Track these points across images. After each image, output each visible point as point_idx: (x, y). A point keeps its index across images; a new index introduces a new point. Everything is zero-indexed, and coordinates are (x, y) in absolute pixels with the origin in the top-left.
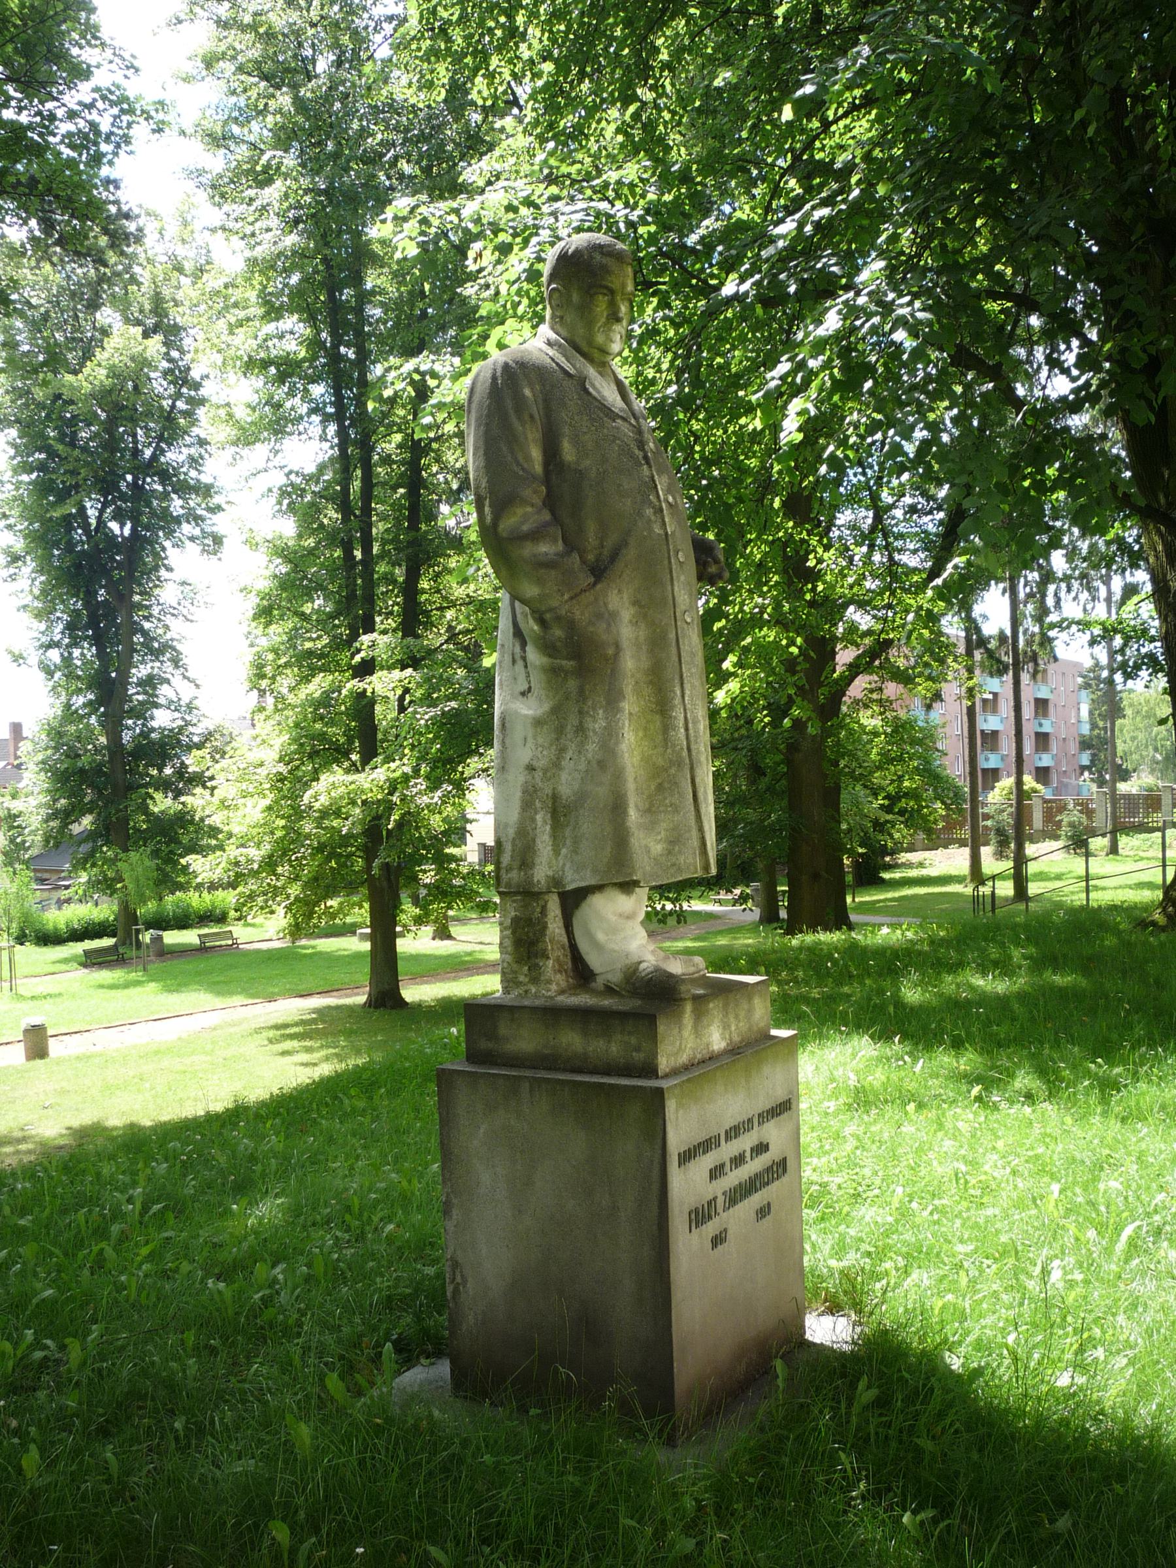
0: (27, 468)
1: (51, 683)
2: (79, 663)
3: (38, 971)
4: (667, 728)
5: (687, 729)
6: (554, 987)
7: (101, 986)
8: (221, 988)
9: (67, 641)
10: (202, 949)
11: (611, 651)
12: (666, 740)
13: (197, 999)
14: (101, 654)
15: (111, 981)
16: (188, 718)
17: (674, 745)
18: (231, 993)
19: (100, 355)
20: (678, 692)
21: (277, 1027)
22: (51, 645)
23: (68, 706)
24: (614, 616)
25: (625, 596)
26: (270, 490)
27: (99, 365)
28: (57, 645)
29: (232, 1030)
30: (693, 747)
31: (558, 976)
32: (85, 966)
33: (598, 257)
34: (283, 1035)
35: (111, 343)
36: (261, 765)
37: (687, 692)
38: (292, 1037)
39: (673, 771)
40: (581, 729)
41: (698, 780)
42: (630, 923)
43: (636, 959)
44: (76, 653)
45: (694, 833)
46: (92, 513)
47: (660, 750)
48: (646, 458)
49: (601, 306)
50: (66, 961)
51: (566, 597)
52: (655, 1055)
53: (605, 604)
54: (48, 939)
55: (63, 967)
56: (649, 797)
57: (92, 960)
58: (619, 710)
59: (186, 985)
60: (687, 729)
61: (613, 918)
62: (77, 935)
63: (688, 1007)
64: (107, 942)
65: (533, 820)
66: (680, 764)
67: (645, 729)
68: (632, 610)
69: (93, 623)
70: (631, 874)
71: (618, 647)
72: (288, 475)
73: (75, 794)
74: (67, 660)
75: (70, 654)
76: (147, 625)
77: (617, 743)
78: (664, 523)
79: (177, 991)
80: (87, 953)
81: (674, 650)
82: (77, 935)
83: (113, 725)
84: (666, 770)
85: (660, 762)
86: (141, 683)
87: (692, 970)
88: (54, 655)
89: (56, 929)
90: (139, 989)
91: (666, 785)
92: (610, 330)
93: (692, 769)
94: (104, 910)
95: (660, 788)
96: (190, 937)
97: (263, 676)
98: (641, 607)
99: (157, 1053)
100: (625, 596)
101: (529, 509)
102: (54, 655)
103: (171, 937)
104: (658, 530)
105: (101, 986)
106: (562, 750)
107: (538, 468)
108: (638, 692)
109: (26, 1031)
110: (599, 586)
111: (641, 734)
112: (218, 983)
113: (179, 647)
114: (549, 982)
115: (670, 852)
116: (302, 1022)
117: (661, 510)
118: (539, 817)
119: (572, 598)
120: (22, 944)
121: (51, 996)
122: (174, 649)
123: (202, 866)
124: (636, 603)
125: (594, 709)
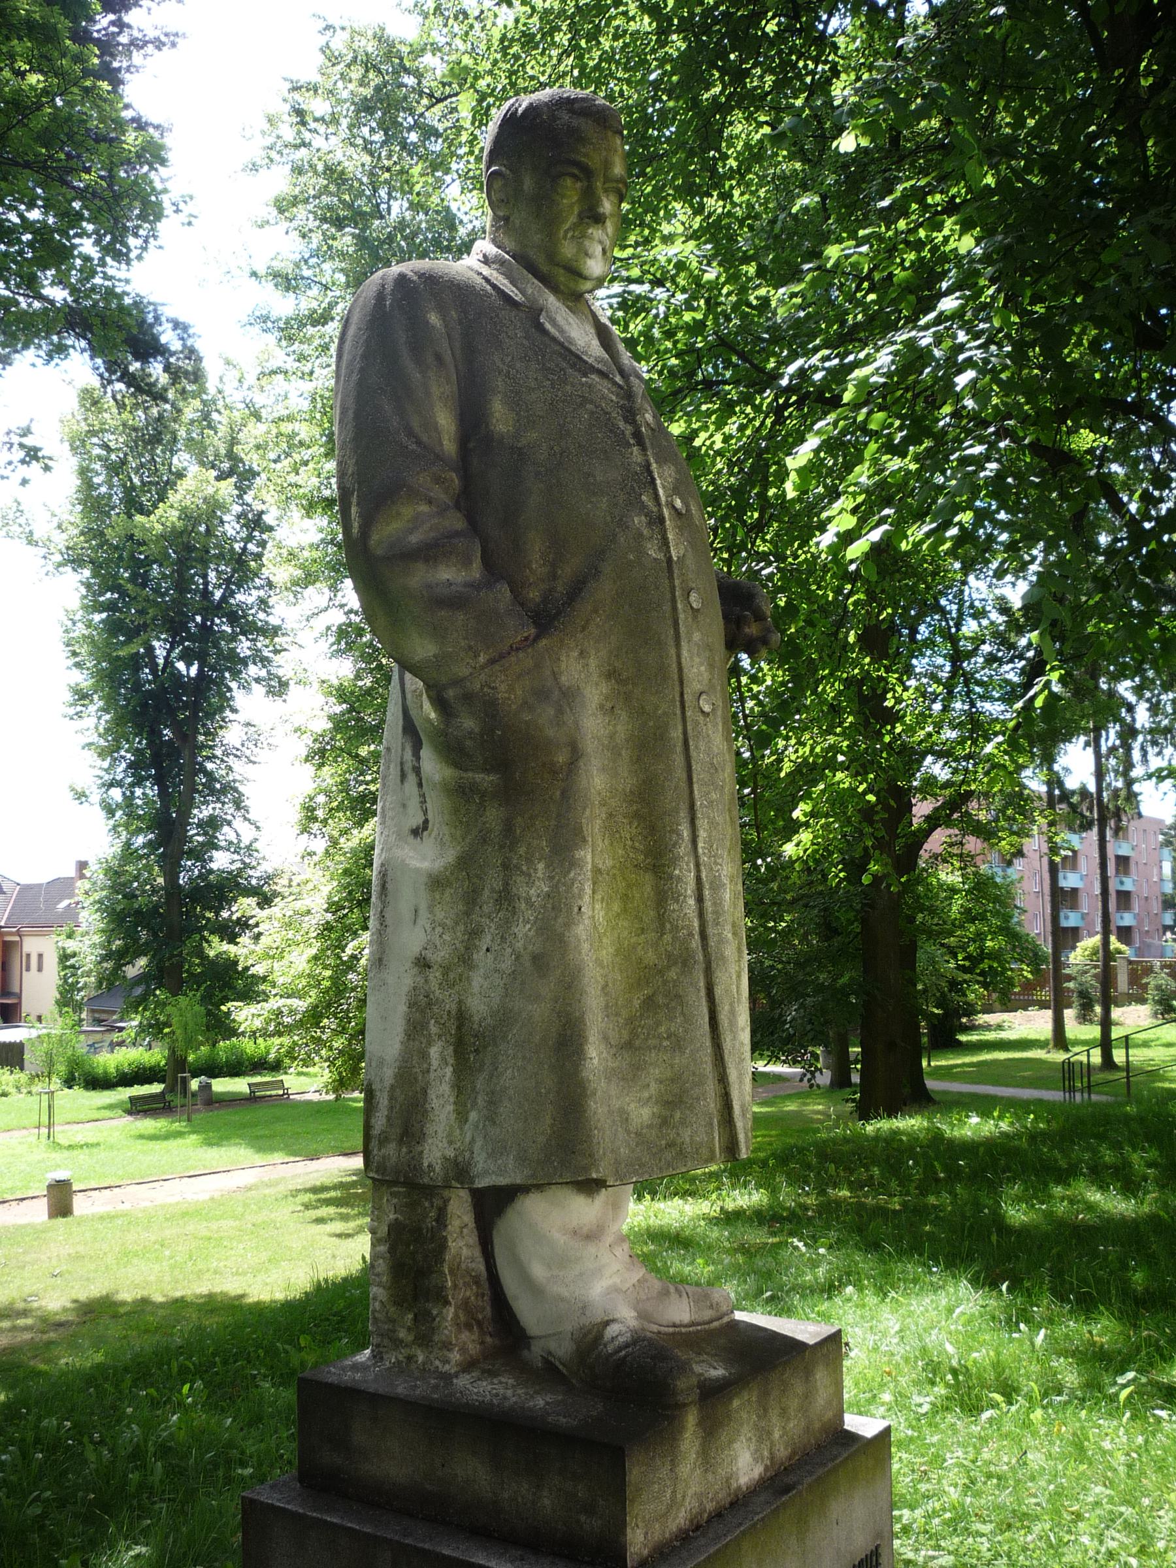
0: (98, 607)
1: (112, 822)
2: (139, 802)
3: (82, 1117)
4: (663, 896)
5: (700, 899)
6: (455, 1356)
7: (141, 1137)
8: (262, 1144)
9: (130, 780)
10: (251, 1099)
11: (561, 758)
12: (661, 919)
13: (238, 1153)
14: (163, 794)
15: (152, 1131)
16: (247, 860)
17: (675, 929)
18: (272, 1149)
19: (173, 497)
20: (686, 834)
21: (315, 1190)
22: (111, 784)
23: (128, 844)
24: (570, 696)
25: (593, 662)
26: (328, 628)
27: (172, 507)
28: (119, 784)
29: (267, 1191)
30: (711, 931)
31: (465, 1336)
32: (130, 1112)
33: (565, 116)
34: (319, 1200)
35: (183, 485)
36: (309, 912)
37: (702, 834)
38: (328, 1202)
39: (673, 974)
40: (506, 898)
41: (718, 991)
42: (592, 1249)
43: (599, 1317)
44: (138, 792)
45: (711, 1087)
46: (160, 653)
47: (652, 936)
48: (637, 435)
49: (570, 196)
50: (111, 1107)
51: (482, 659)
52: (622, 1526)
53: (555, 676)
54: (97, 1082)
55: (107, 1113)
56: (630, 1021)
57: (138, 1107)
58: (574, 864)
59: (228, 1138)
60: (700, 899)
61: (560, 1238)
62: (127, 1079)
63: (691, 1419)
64: (156, 1088)
65: (424, 1056)
66: (685, 961)
67: (625, 898)
68: (604, 688)
69: (156, 761)
70: (586, 1169)
71: (576, 753)
72: (347, 613)
73: (130, 935)
74: (129, 799)
75: (132, 793)
76: (210, 766)
77: (568, 925)
78: (665, 542)
79: (218, 1145)
80: (133, 1100)
81: (679, 760)
82: (127, 1079)
83: (171, 867)
84: (661, 972)
85: (651, 957)
86: (200, 825)
87: (708, 1314)
88: (116, 794)
89: (105, 1072)
90: (180, 1141)
91: (661, 1000)
92: (583, 236)
93: (708, 971)
94: (156, 1056)
95: (649, 1003)
96: (239, 1085)
97: (315, 819)
98: (619, 681)
99: (184, 1214)
100: (593, 662)
101: (424, 508)
102: (116, 794)
103: (221, 1085)
104: (653, 551)
105: (141, 1137)
106: (475, 933)
107: (449, 446)
108: (611, 830)
109: (50, 1187)
110: (544, 642)
111: (616, 907)
112: (261, 1137)
113: (241, 788)
114: (447, 1346)
115: (664, 1122)
116: (341, 1186)
117: (661, 520)
118: (434, 1052)
119: (492, 662)
120: (70, 1087)
121: (87, 1145)
122: (236, 790)
123: (245, 1015)
124: (611, 674)
125: (529, 861)
